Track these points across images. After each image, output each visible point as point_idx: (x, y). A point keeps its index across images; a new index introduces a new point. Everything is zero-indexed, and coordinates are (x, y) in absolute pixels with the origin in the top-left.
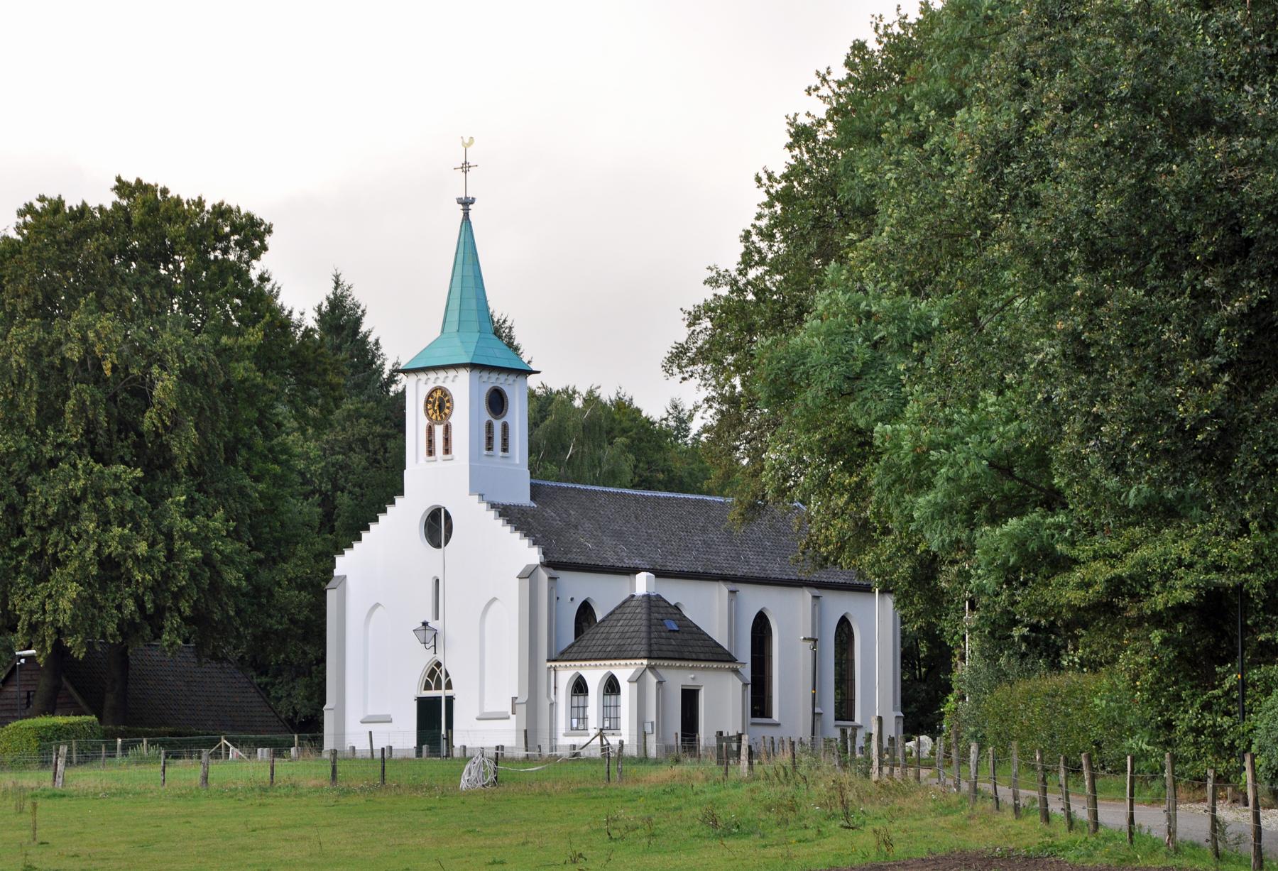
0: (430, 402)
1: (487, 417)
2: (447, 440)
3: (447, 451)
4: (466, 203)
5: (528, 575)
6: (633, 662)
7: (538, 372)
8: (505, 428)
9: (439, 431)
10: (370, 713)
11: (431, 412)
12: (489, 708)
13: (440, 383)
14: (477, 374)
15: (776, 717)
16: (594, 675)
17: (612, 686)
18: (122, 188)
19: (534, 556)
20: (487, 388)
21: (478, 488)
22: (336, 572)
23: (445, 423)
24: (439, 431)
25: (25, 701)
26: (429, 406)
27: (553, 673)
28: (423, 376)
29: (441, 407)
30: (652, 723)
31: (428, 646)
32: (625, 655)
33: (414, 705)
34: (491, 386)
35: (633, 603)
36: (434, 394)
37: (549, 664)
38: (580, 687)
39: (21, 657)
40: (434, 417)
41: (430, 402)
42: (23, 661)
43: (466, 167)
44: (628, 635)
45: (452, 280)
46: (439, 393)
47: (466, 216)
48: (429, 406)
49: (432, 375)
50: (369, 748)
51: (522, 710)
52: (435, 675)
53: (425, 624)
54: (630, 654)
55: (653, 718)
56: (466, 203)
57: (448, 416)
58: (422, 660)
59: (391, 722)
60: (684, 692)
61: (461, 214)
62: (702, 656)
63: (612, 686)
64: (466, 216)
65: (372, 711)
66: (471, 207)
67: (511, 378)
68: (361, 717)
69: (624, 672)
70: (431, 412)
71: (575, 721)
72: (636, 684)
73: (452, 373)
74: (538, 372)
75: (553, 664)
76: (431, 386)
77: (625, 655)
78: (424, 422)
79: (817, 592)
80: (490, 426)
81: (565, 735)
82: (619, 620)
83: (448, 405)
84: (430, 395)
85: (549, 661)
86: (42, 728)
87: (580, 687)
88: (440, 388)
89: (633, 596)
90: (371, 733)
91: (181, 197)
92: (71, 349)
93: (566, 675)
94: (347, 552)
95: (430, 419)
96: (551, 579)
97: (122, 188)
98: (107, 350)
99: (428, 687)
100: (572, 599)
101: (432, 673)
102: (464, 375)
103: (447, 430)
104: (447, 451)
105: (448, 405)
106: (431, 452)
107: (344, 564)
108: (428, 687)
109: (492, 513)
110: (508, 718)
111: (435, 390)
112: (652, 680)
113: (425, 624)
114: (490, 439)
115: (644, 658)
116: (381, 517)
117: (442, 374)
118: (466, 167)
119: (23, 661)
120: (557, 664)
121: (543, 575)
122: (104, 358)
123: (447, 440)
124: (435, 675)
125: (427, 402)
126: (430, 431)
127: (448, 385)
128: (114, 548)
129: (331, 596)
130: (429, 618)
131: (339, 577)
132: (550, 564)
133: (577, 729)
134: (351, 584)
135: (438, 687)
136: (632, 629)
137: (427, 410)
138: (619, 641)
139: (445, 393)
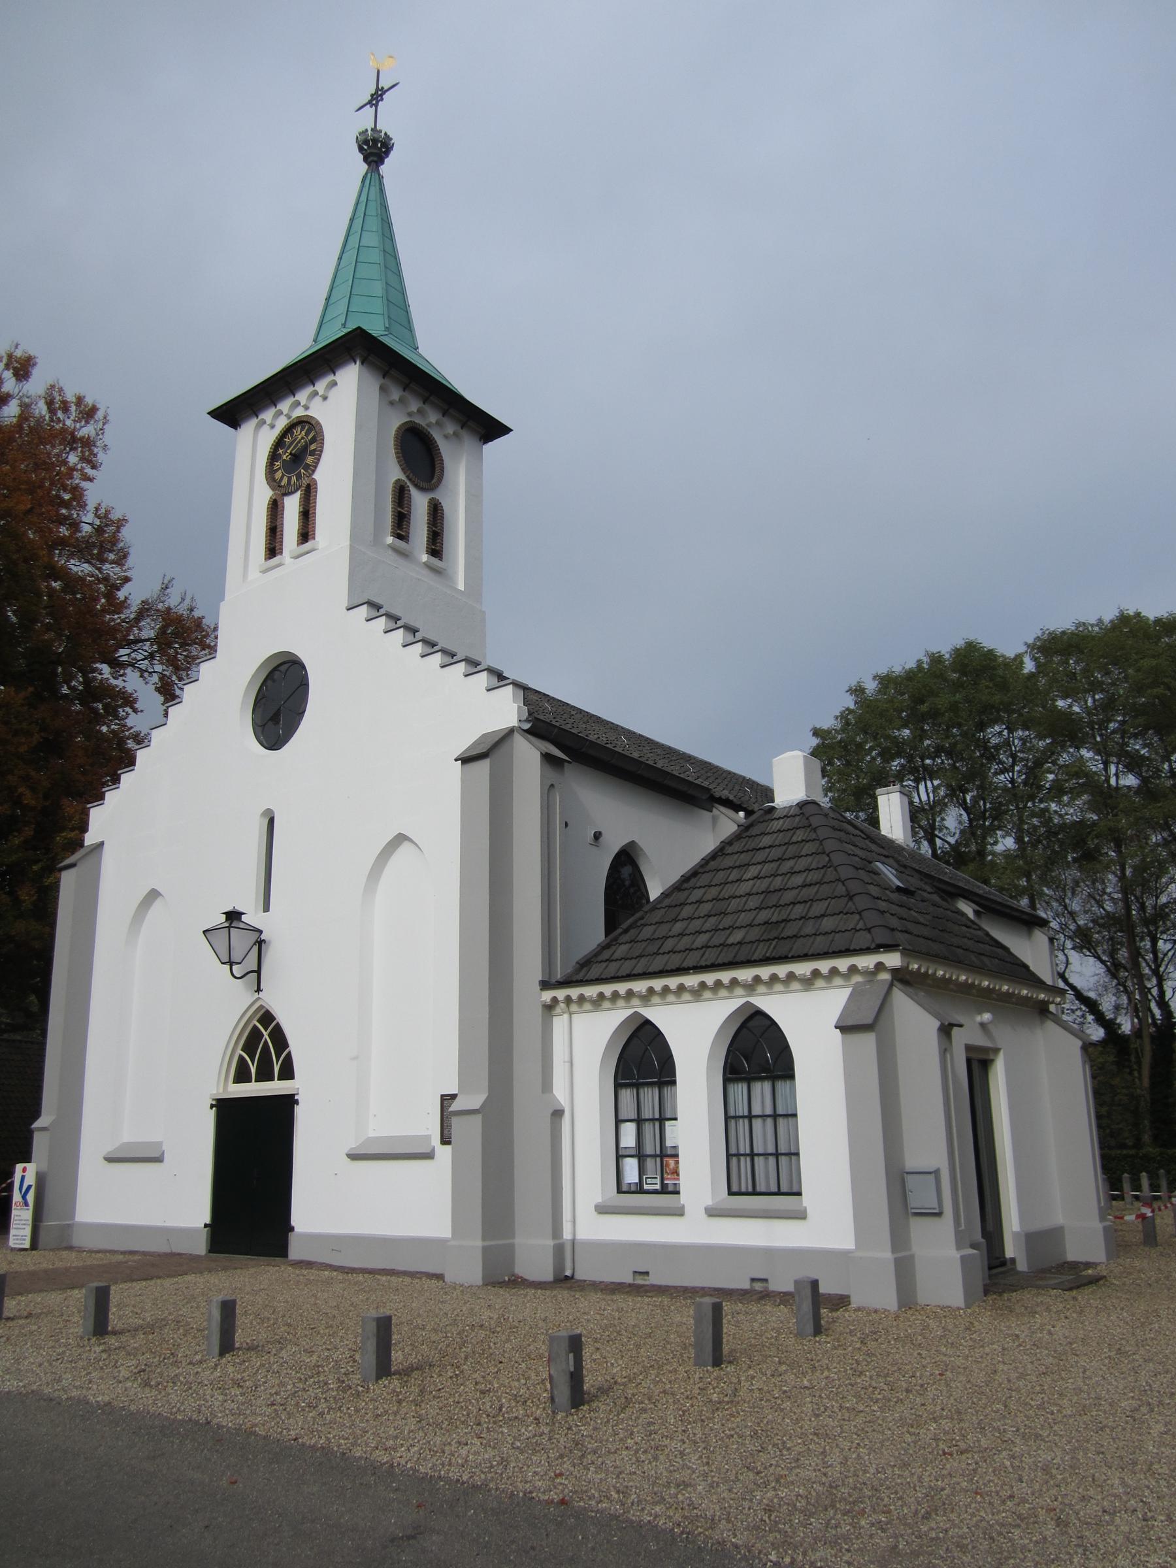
1: (395, 473)
2: (307, 515)
3: (305, 535)
6: (843, 964)
8: (436, 513)
13: (299, 412)
20: (397, 421)
22: (90, 839)
24: (292, 505)
33: (210, 1117)
34: (406, 419)
37: (547, 996)
43: (377, 97)
44: (788, 896)
45: (340, 259)
51: (469, 1131)
53: (233, 916)
59: (159, 1160)
71: (631, 1167)
72: (868, 1041)
77: (799, 946)
78: (264, 494)
80: (401, 495)
81: (602, 1210)
85: (545, 985)
99: (242, 1076)
100: (597, 836)
101: (252, 1042)
106: (273, 550)
110: (429, 1156)
113: (233, 916)
115: (889, 947)
118: (377, 97)
123: (307, 515)
126: (275, 509)
129: (68, 881)
133: (639, 1190)
136: (798, 880)
138: (763, 916)
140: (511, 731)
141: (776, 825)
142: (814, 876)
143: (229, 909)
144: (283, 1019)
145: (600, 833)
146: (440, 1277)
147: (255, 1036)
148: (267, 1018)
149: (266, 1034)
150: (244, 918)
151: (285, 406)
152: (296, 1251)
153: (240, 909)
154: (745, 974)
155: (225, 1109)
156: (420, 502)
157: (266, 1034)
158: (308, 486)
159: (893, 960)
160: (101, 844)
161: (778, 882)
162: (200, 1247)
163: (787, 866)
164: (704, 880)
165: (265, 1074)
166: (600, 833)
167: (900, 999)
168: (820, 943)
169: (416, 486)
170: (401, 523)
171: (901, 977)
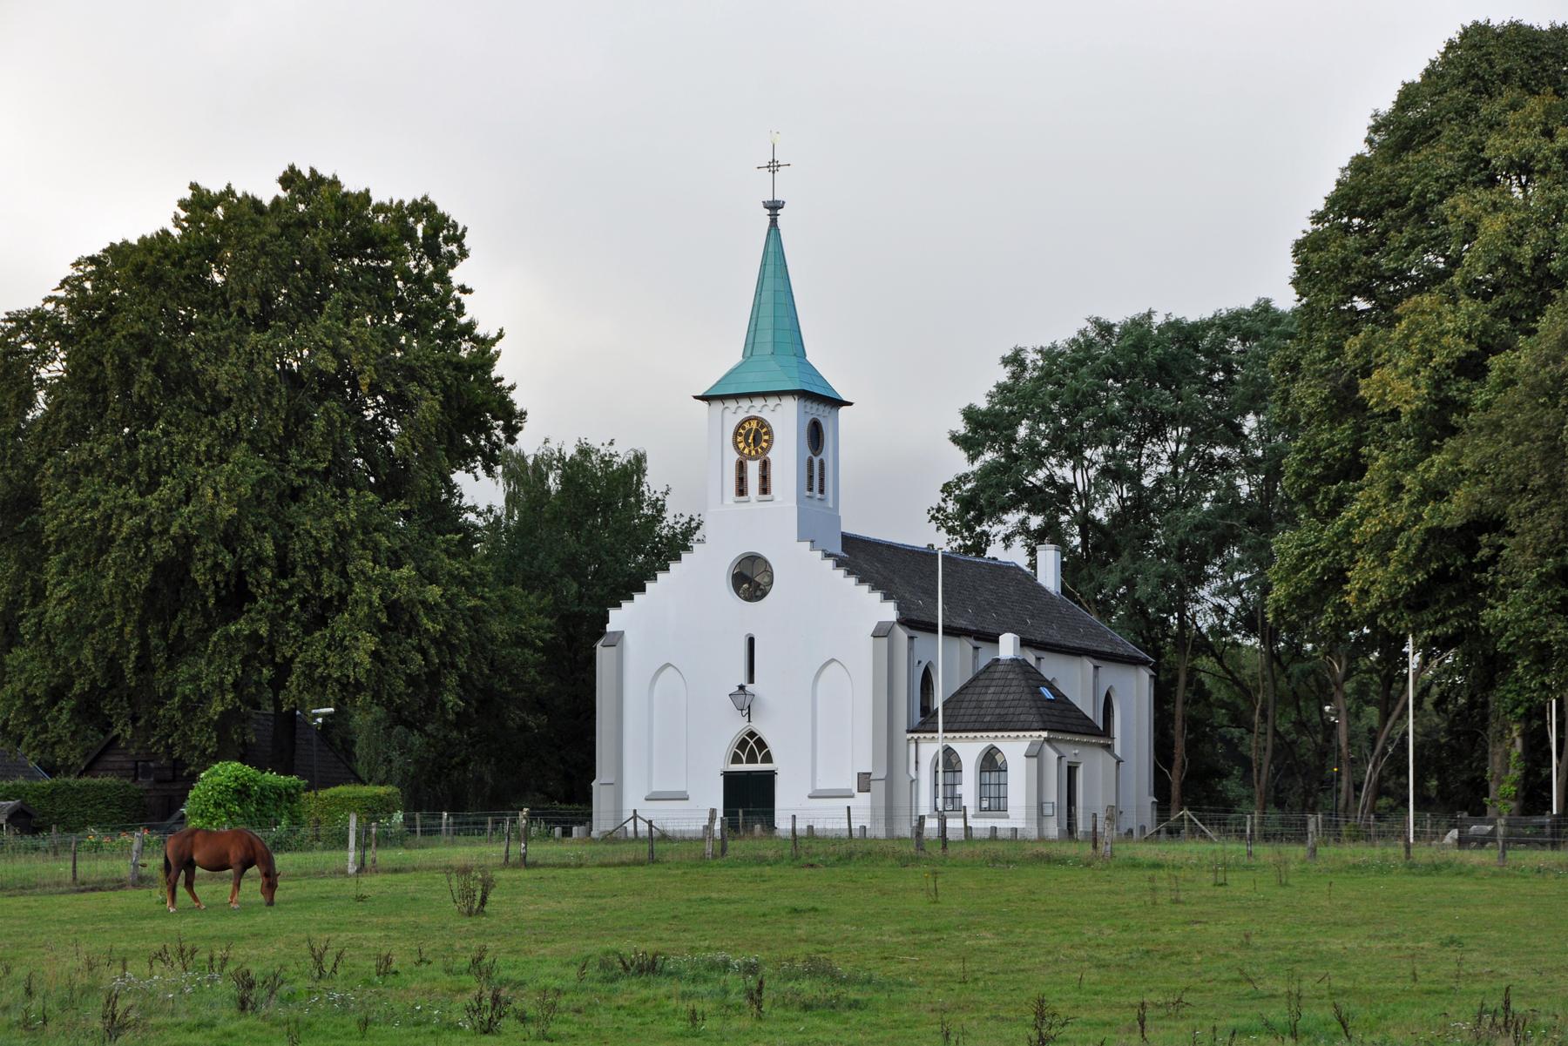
0: (741, 435)
3: (765, 490)
4: (774, 207)
5: (882, 632)
6: (1028, 734)
7: (850, 404)
8: (822, 463)
9: (753, 468)
10: (654, 789)
11: (741, 446)
12: (823, 785)
13: (753, 413)
16: (970, 749)
17: (991, 763)
18: (290, 179)
19: (889, 612)
21: (807, 533)
22: (610, 628)
23: (763, 458)
24: (753, 468)
25: (133, 773)
26: (739, 439)
27: (913, 746)
28: (732, 405)
29: (757, 440)
35: (1001, 668)
36: (747, 426)
37: (909, 736)
38: (950, 762)
39: (317, 716)
40: (746, 451)
41: (741, 435)
42: (320, 720)
43: (773, 166)
44: (1007, 704)
46: (754, 425)
47: (774, 223)
48: (739, 439)
49: (745, 404)
50: (846, 826)
51: (879, 788)
52: (751, 745)
54: (1019, 725)
55: (1054, 799)
56: (774, 207)
57: (766, 450)
58: (736, 727)
60: (1069, 768)
61: (768, 219)
62: (1081, 730)
63: (991, 763)
64: (774, 223)
65: (658, 787)
66: (779, 212)
68: (646, 794)
69: (1014, 748)
70: (741, 446)
73: (772, 402)
74: (850, 404)
75: (916, 736)
76: (742, 416)
78: (733, 457)
79: (1097, 663)
80: (811, 462)
82: (988, 687)
83: (766, 437)
84: (741, 425)
85: (909, 731)
86: (368, 797)
87: (950, 762)
88: (755, 418)
89: (998, 660)
90: (849, 808)
91: (371, 194)
92: (323, 359)
93: (930, 748)
94: (625, 604)
95: (741, 452)
96: (911, 638)
97: (290, 179)
98: (365, 362)
101: (742, 744)
102: (791, 406)
103: (765, 466)
104: (765, 490)
105: (766, 437)
106: (741, 491)
107: (618, 619)
108: (736, 759)
109: (830, 563)
110: (852, 797)
111: (749, 419)
112: (1051, 755)
113: (742, 687)
114: (811, 477)
115: (1044, 730)
116: (673, 566)
117: (759, 403)
119: (320, 720)
120: (922, 735)
121: (902, 634)
122: (362, 372)
124: (751, 745)
125: (736, 434)
126: (741, 467)
127: (766, 415)
128: (403, 592)
129: (603, 654)
130: (743, 680)
131: (614, 633)
132: (905, 622)
134: (630, 640)
135: (752, 759)
136: (1011, 697)
137: (736, 444)
138: (997, 711)
139: (762, 423)
141: (1001, 668)
142: (1017, 696)
149: (752, 742)
154: (992, 734)
155: (729, 778)
157: (752, 742)
159: (1045, 734)
161: (1002, 697)
163: (1006, 689)
164: (971, 690)
167: (1047, 747)
168: (1019, 725)
171: (1047, 740)
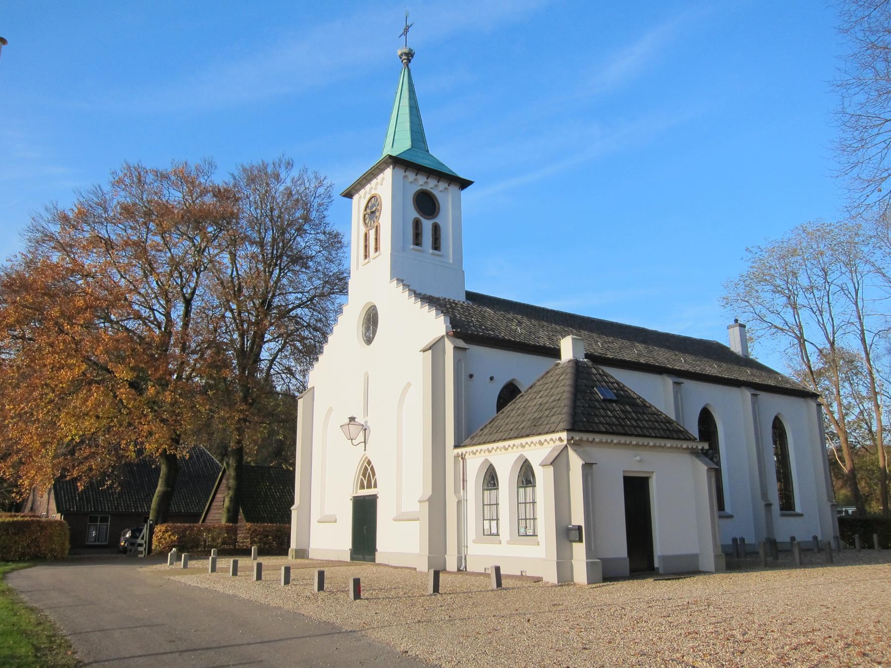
1: (414, 214)
3: (376, 249)
5: (435, 348)
8: (436, 229)
13: (373, 192)
14: (401, 172)
15: (798, 509)
24: (372, 233)
30: (580, 528)
31: (355, 442)
32: (540, 431)
34: (419, 188)
38: (491, 479)
52: (368, 475)
53: (352, 419)
59: (335, 521)
63: (526, 476)
67: (442, 185)
78: (363, 229)
80: (417, 225)
81: (475, 541)
87: (491, 479)
99: (362, 487)
100: (492, 379)
106: (366, 257)
112: (576, 462)
113: (352, 419)
140: (443, 337)
143: (350, 416)
144: (373, 463)
145: (493, 377)
146: (415, 569)
147: (366, 469)
148: (369, 463)
150: (356, 420)
151: (368, 187)
152: (379, 558)
153: (354, 416)
156: (427, 225)
158: (377, 226)
160: (313, 388)
162: (347, 558)
165: (369, 486)
166: (493, 377)
169: (425, 218)
170: (417, 239)
